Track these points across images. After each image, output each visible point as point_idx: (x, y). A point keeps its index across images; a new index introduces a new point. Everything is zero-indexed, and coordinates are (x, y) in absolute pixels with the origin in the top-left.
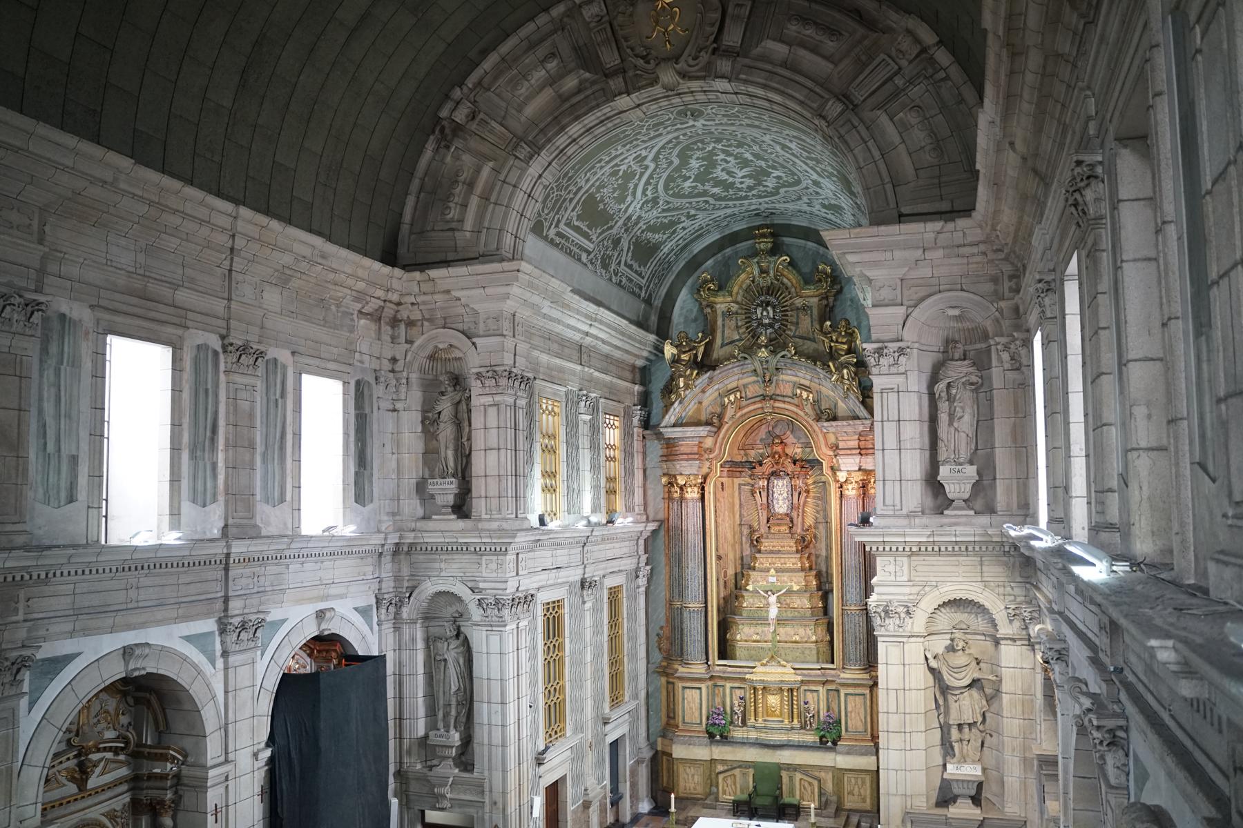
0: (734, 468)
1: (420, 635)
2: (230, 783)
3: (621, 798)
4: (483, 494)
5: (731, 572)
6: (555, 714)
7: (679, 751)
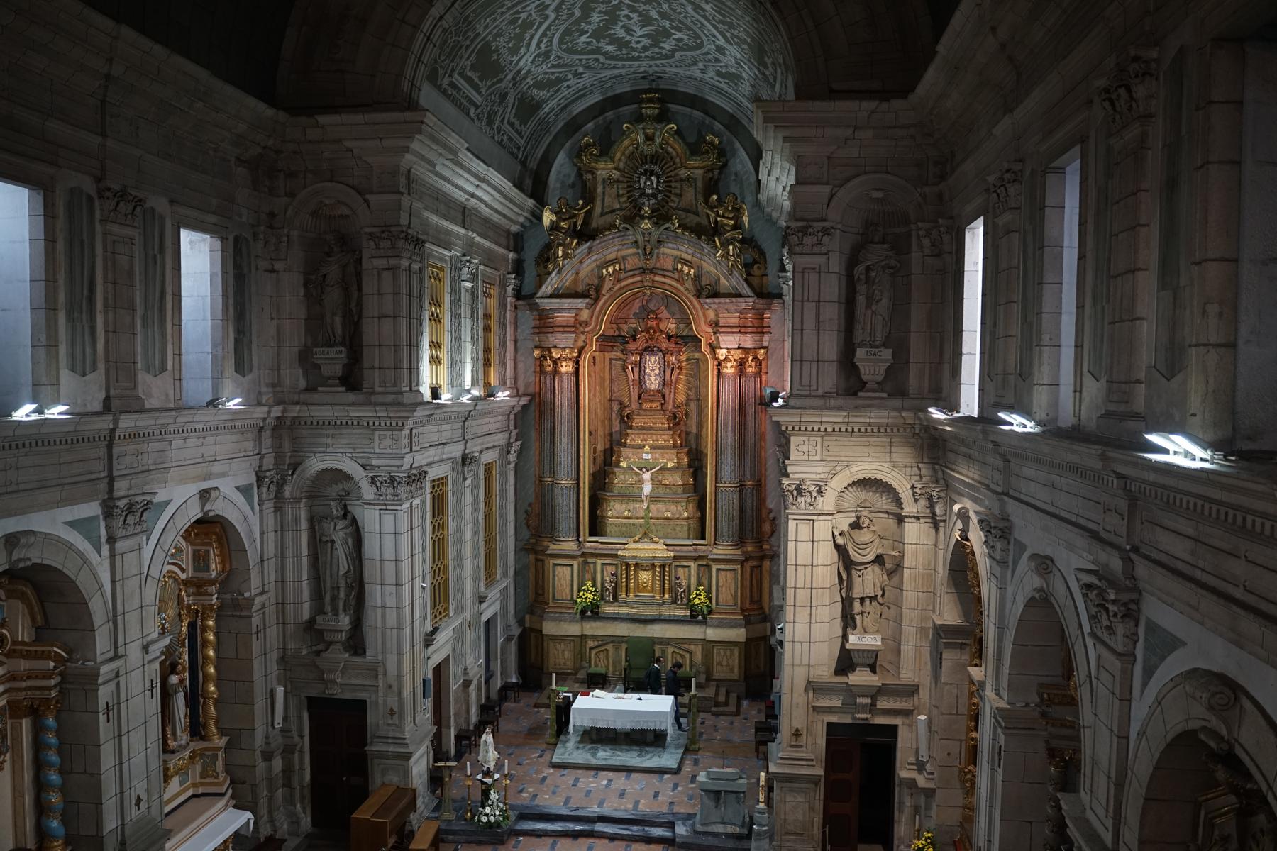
0: (607, 342)
1: (303, 515)
2: (122, 679)
3: (492, 676)
4: (376, 365)
5: (600, 448)
6: (440, 594)
7: (549, 628)
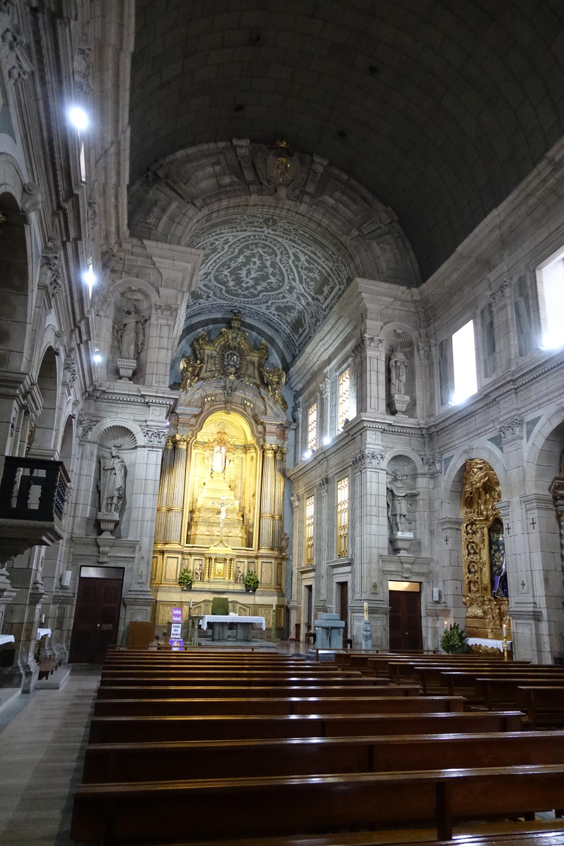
4: (155, 372)
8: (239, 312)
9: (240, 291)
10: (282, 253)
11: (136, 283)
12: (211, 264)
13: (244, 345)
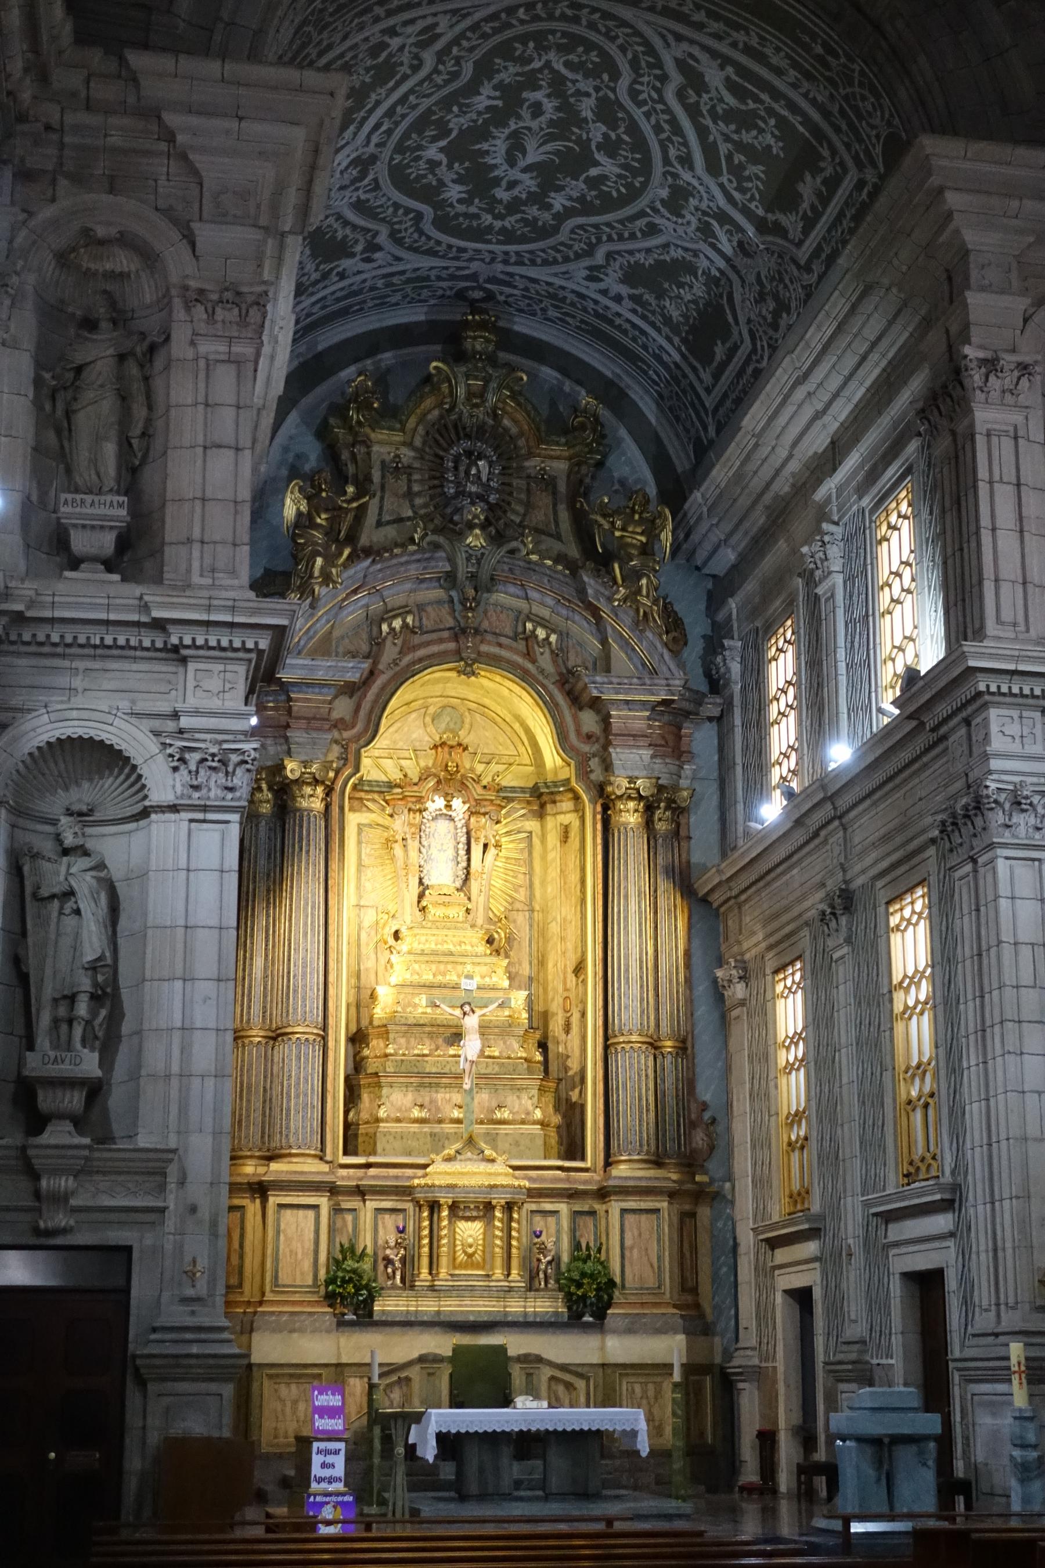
4: (197, 534)
8: (490, 297)
9: (487, 219)
10: (634, 64)
11: (112, 212)
12: (377, 126)
13: (515, 421)
